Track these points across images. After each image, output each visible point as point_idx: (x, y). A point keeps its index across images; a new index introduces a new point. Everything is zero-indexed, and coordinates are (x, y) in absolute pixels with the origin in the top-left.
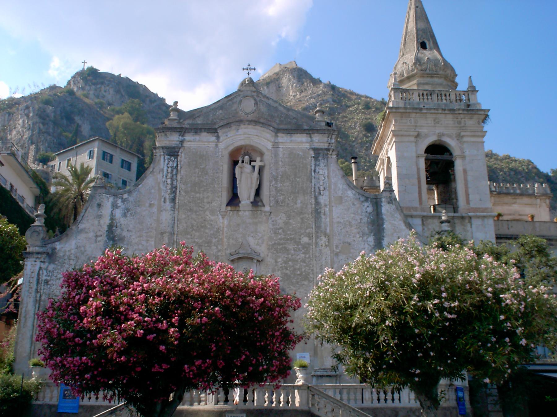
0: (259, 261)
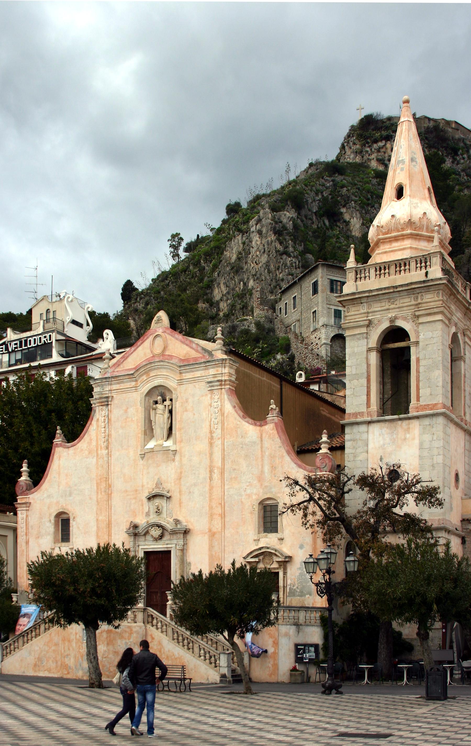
0: (169, 498)
